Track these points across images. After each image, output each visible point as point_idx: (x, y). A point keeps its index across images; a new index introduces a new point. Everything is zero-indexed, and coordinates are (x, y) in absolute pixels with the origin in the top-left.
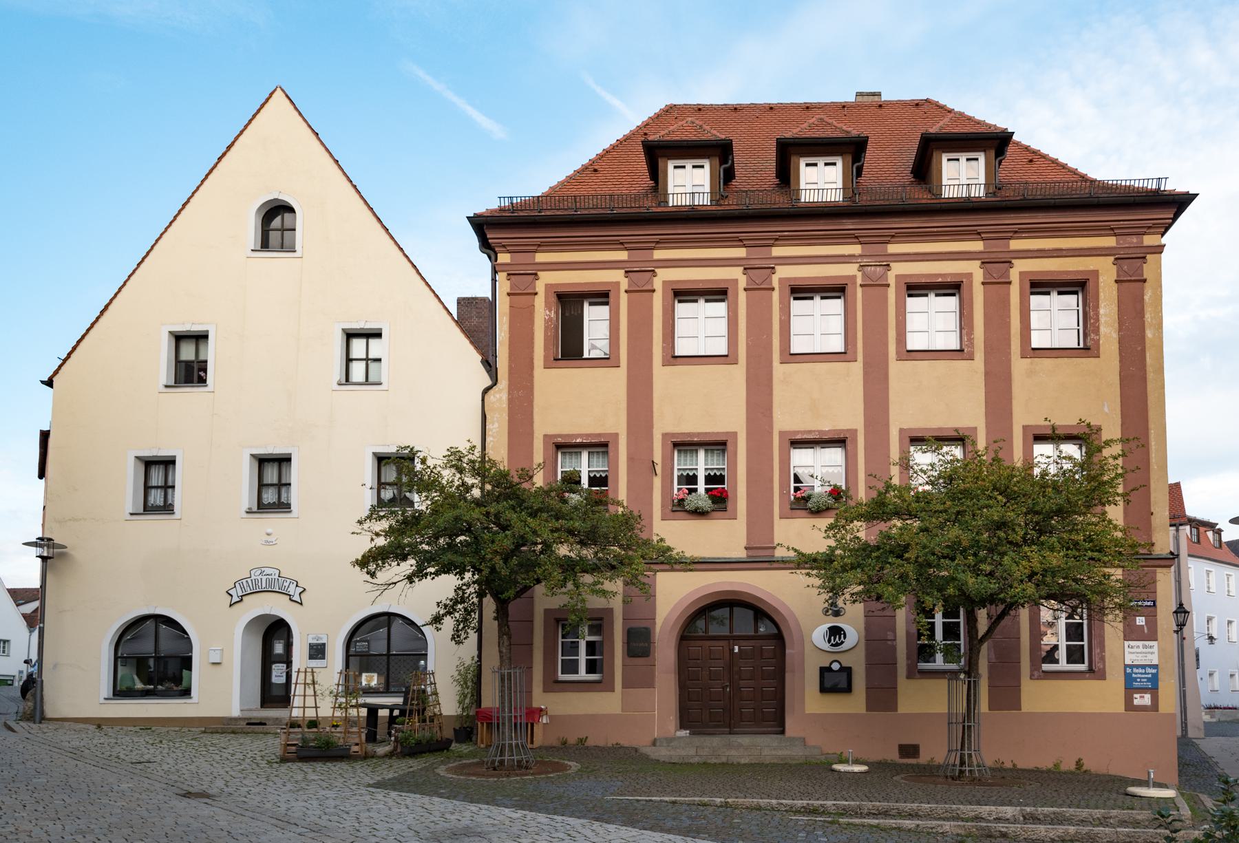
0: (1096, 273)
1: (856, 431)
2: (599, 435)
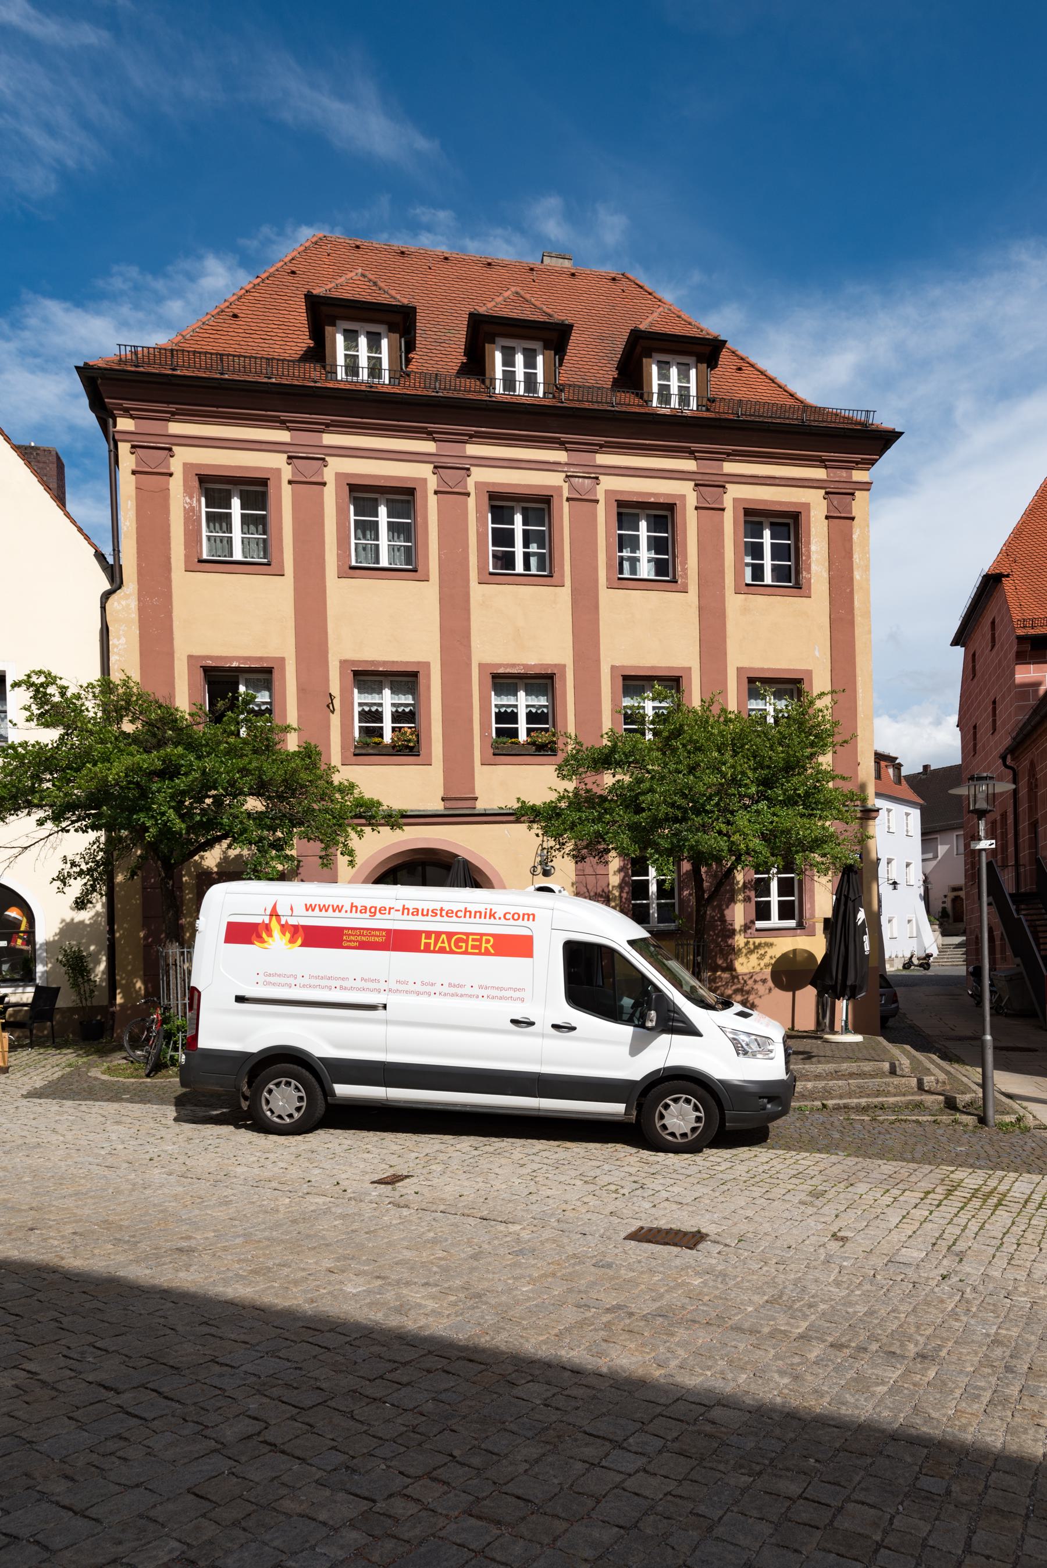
0: (807, 506)
1: (564, 666)
2: (261, 659)
